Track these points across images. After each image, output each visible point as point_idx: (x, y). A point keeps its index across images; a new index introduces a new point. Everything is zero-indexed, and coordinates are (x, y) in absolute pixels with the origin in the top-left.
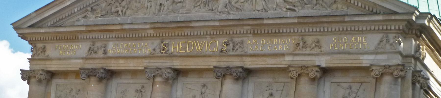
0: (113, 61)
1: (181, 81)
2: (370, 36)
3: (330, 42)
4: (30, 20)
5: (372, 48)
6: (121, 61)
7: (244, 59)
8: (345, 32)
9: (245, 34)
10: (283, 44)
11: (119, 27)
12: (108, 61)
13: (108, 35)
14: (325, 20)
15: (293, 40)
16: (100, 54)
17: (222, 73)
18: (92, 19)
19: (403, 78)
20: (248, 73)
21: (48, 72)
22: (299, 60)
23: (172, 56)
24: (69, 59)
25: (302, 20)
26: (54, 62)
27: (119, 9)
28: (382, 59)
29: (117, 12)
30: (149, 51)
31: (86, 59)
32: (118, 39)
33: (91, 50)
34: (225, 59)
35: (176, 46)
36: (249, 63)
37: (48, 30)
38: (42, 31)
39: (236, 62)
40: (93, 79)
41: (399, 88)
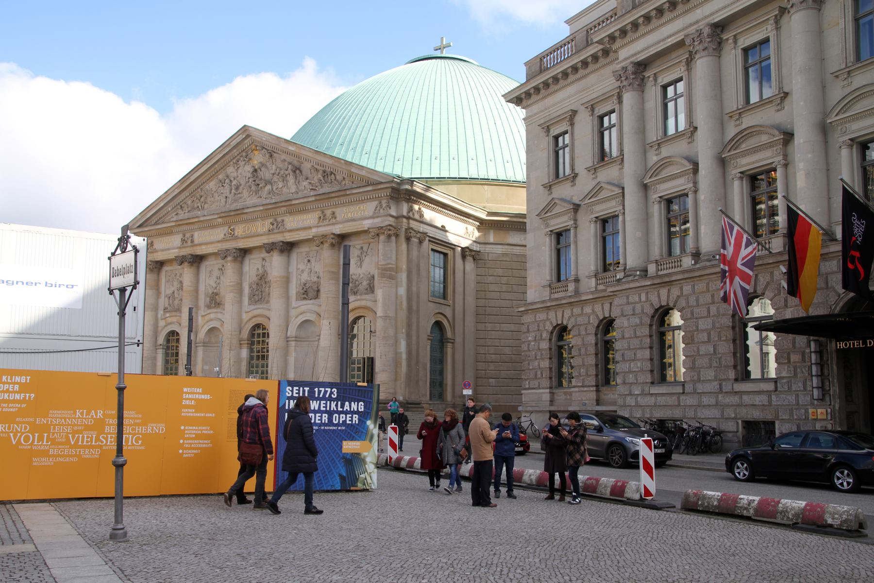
2: (368, 204)
3: (343, 213)
4: (138, 221)
5: (371, 214)
6: (204, 247)
8: (350, 203)
9: (284, 214)
10: (310, 219)
11: (196, 220)
12: (195, 248)
13: (192, 227)
14: (333, 195)
15: (317, 214)
16: (189, 243)
17: (270, 248)
18: (183, 215)
19: (397, 236)
21: (157, 262)
22: (323, 230)
23: (236, 238)
24: (169, 249)
25: (318, 198)
26: (160, 253)
28: (378, 222)
30: (222, 236)
31: (180, 248)
32: (200, 229)
34: (271, 236)
35: (239, 230)
36: (290, 237)
37: (152, 228)
38: (146, 229)
39: (278, 238)
40: (186, 264)
41: (394, 244)
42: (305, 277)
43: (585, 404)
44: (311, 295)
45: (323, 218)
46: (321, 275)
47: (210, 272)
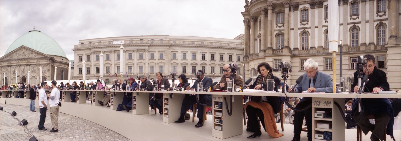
1: (21, 66)
5: (46, 61)
10: (35, 61)
20: (30, 65)
22: (37, 63)
23: (20, 63)
36: (31, 63)
42: (33, 69)
44: (34, 72)
46: (36, 70)
47: (13, 68)
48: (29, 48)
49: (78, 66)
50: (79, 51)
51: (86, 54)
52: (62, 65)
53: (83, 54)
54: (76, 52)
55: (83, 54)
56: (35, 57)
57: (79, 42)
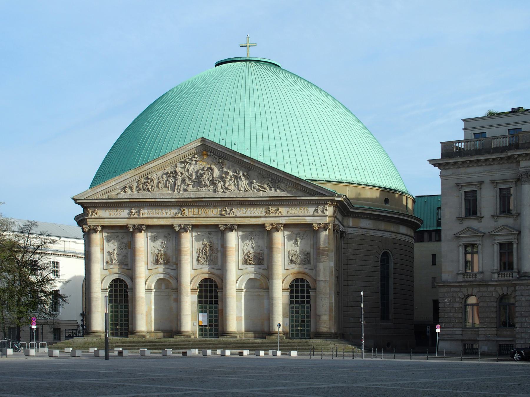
0: (149, 219)
6: (155, 220)
7: (236, 219)
26: (106, 220)
27: (150, 187)
29: (148, 189)
33: (130, 213)
43: (489, 337)
45: (268, 212)
48: (234, 152)
49: (457, 237)
50: (462, 170)
51: (495, 183)
52: (383, 225)
53: (483, 182)
54: (450, 172)
55: (483, 182)
56: (261, 194)
57: (463, 123)
